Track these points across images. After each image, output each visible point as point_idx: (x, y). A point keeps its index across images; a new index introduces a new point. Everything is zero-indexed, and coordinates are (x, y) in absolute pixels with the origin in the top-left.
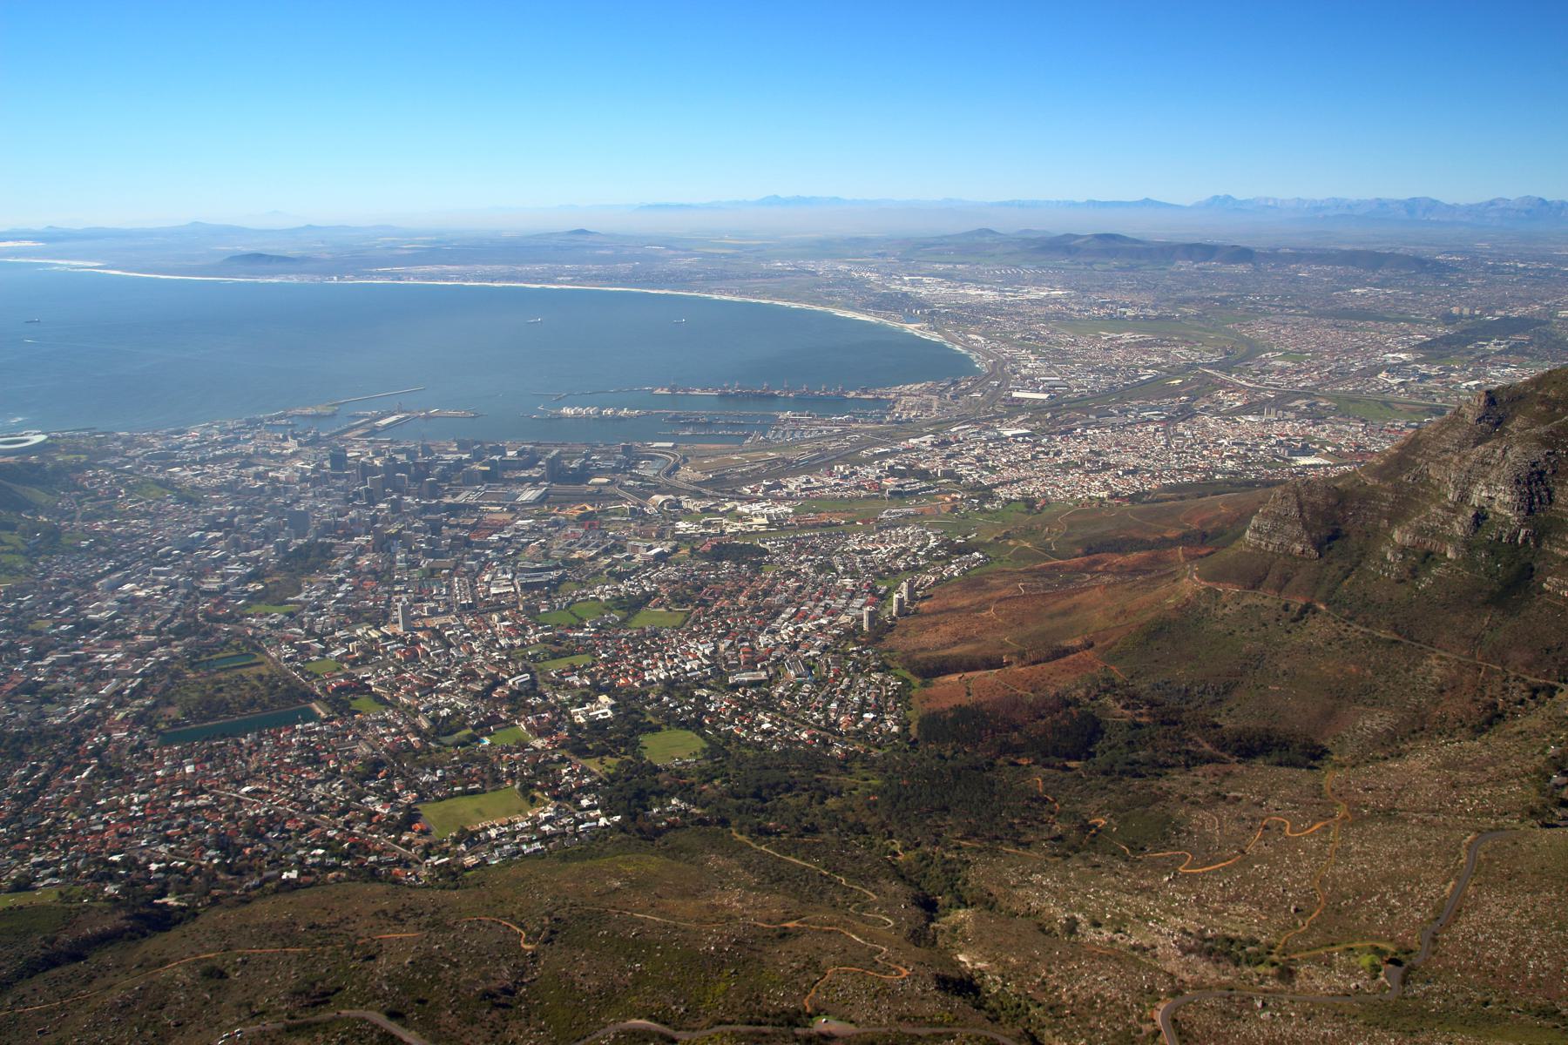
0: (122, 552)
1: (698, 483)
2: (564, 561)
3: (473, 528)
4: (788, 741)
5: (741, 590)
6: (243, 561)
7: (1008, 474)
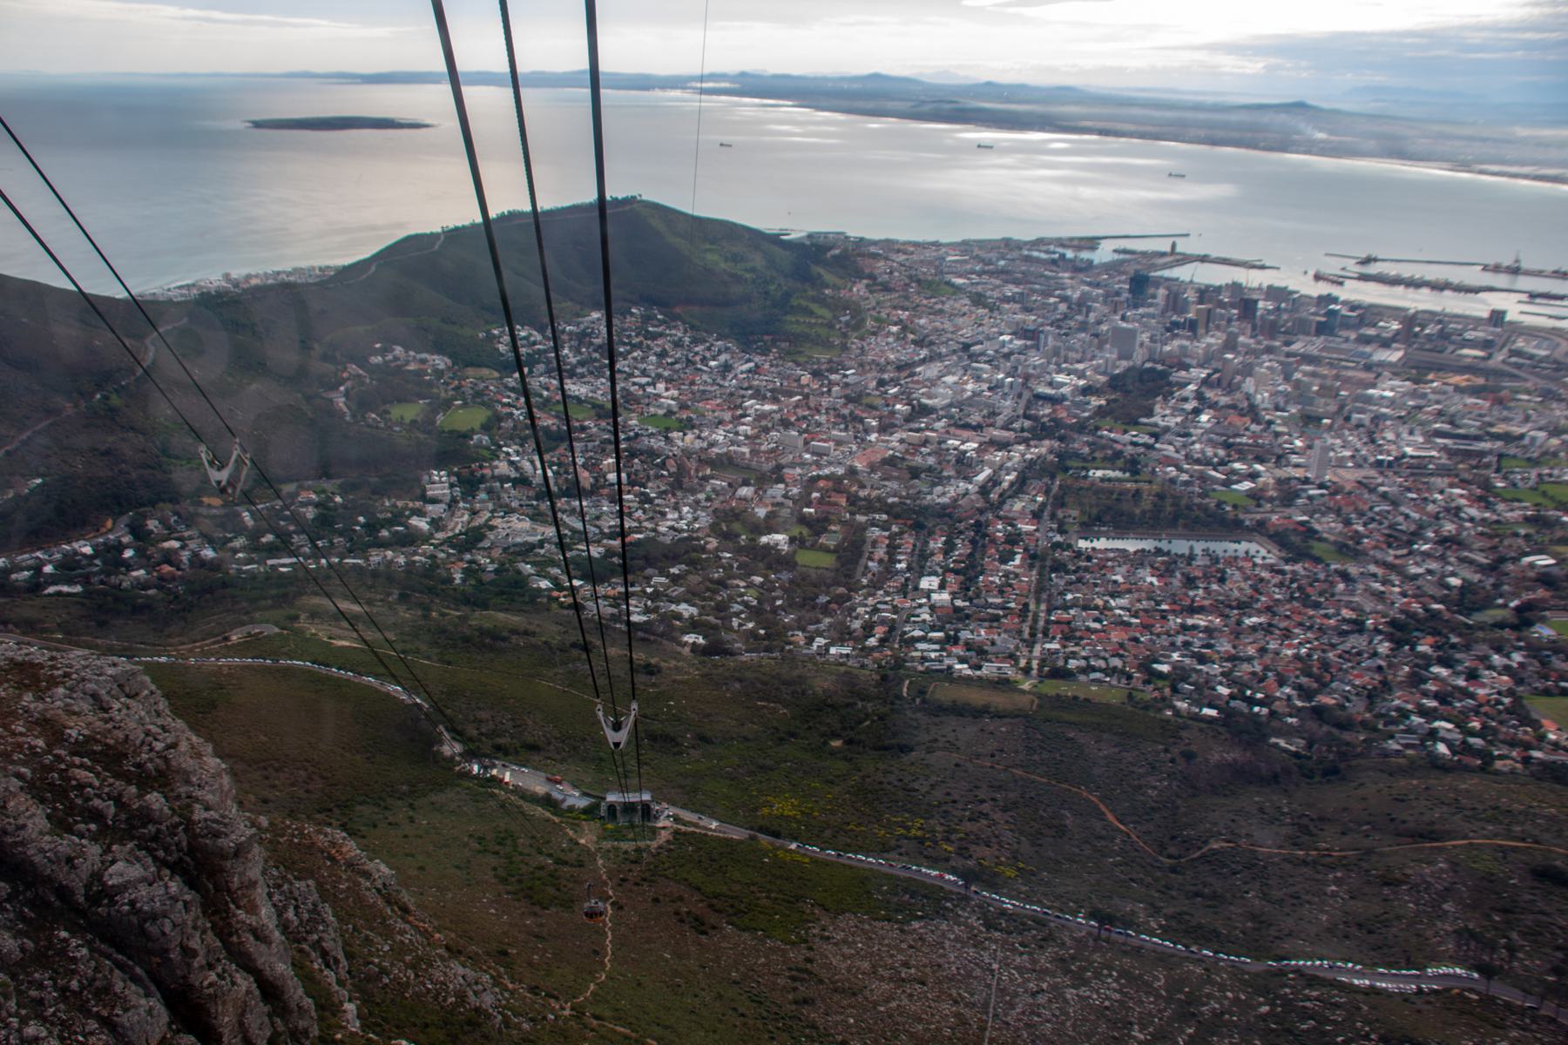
0: (932, 343)
2: (1488, 433)
3: (1337, 377)
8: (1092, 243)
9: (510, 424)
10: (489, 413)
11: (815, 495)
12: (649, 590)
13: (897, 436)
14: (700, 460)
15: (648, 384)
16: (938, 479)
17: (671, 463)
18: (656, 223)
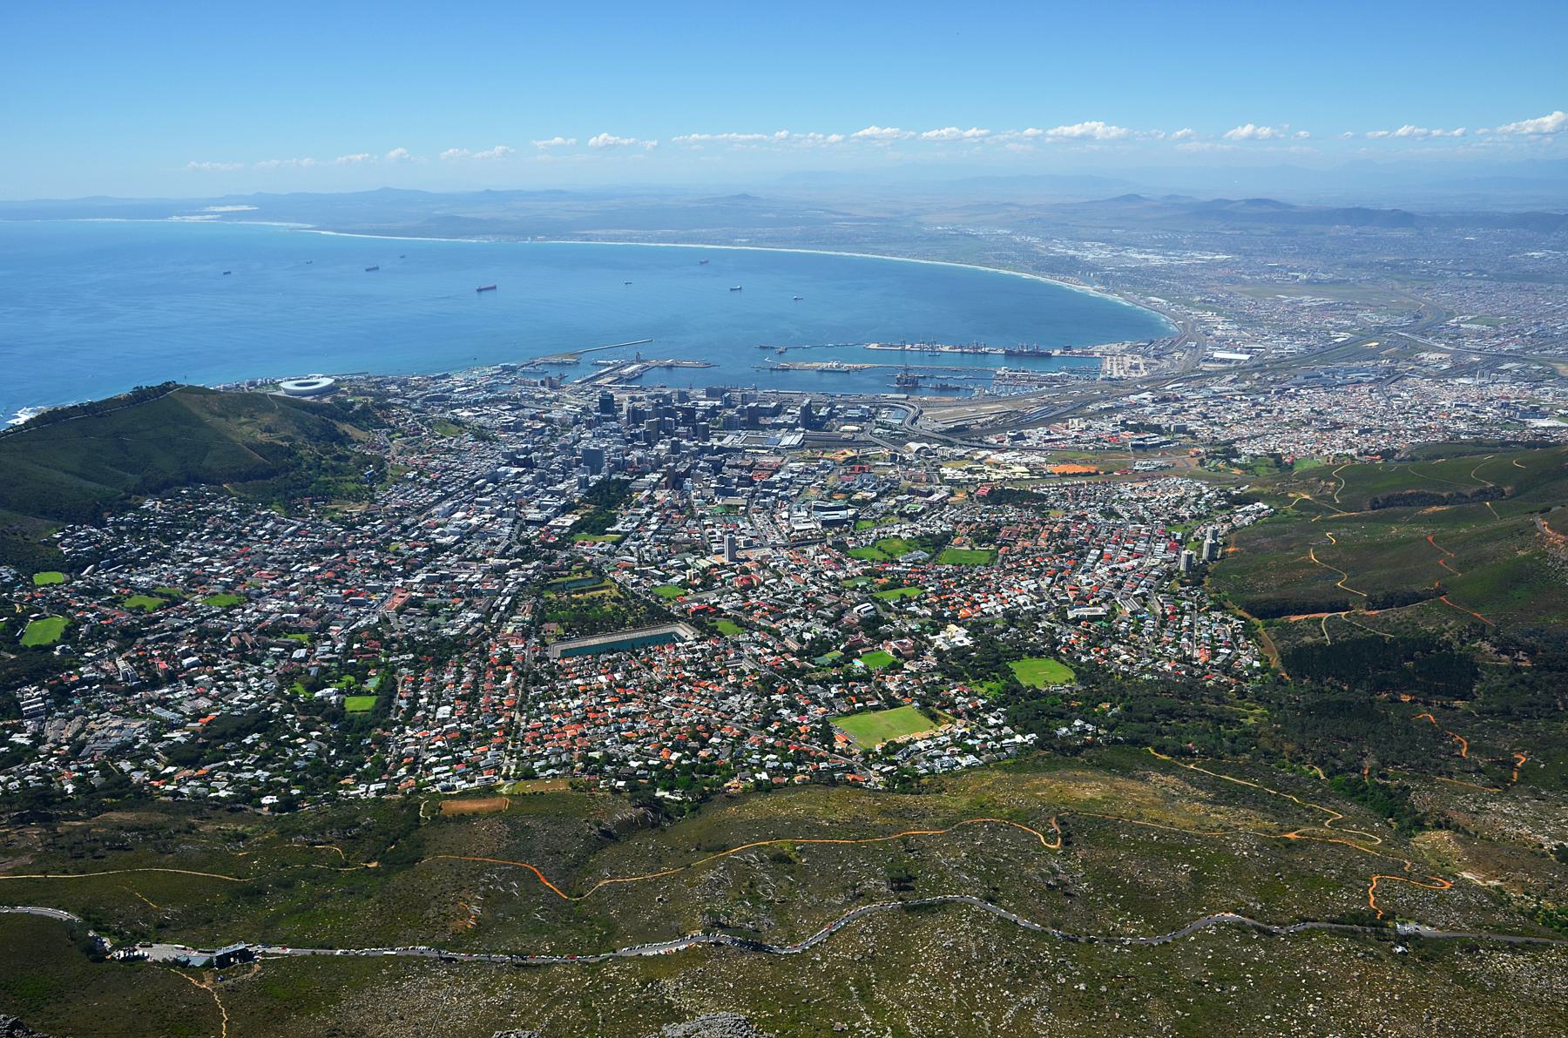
3: (750, 468)
4: (1154, 671)
5: (1035, 532)
6: (553, 494)
7: (1242, 431)
9: (84, 629)
10: (67, 621)
11: (356, 646)
12: (232, 763)
13: (418, 579)
14: (261, 632)
15: (206, 563)
16: (453, 615)
17: (234, 641)
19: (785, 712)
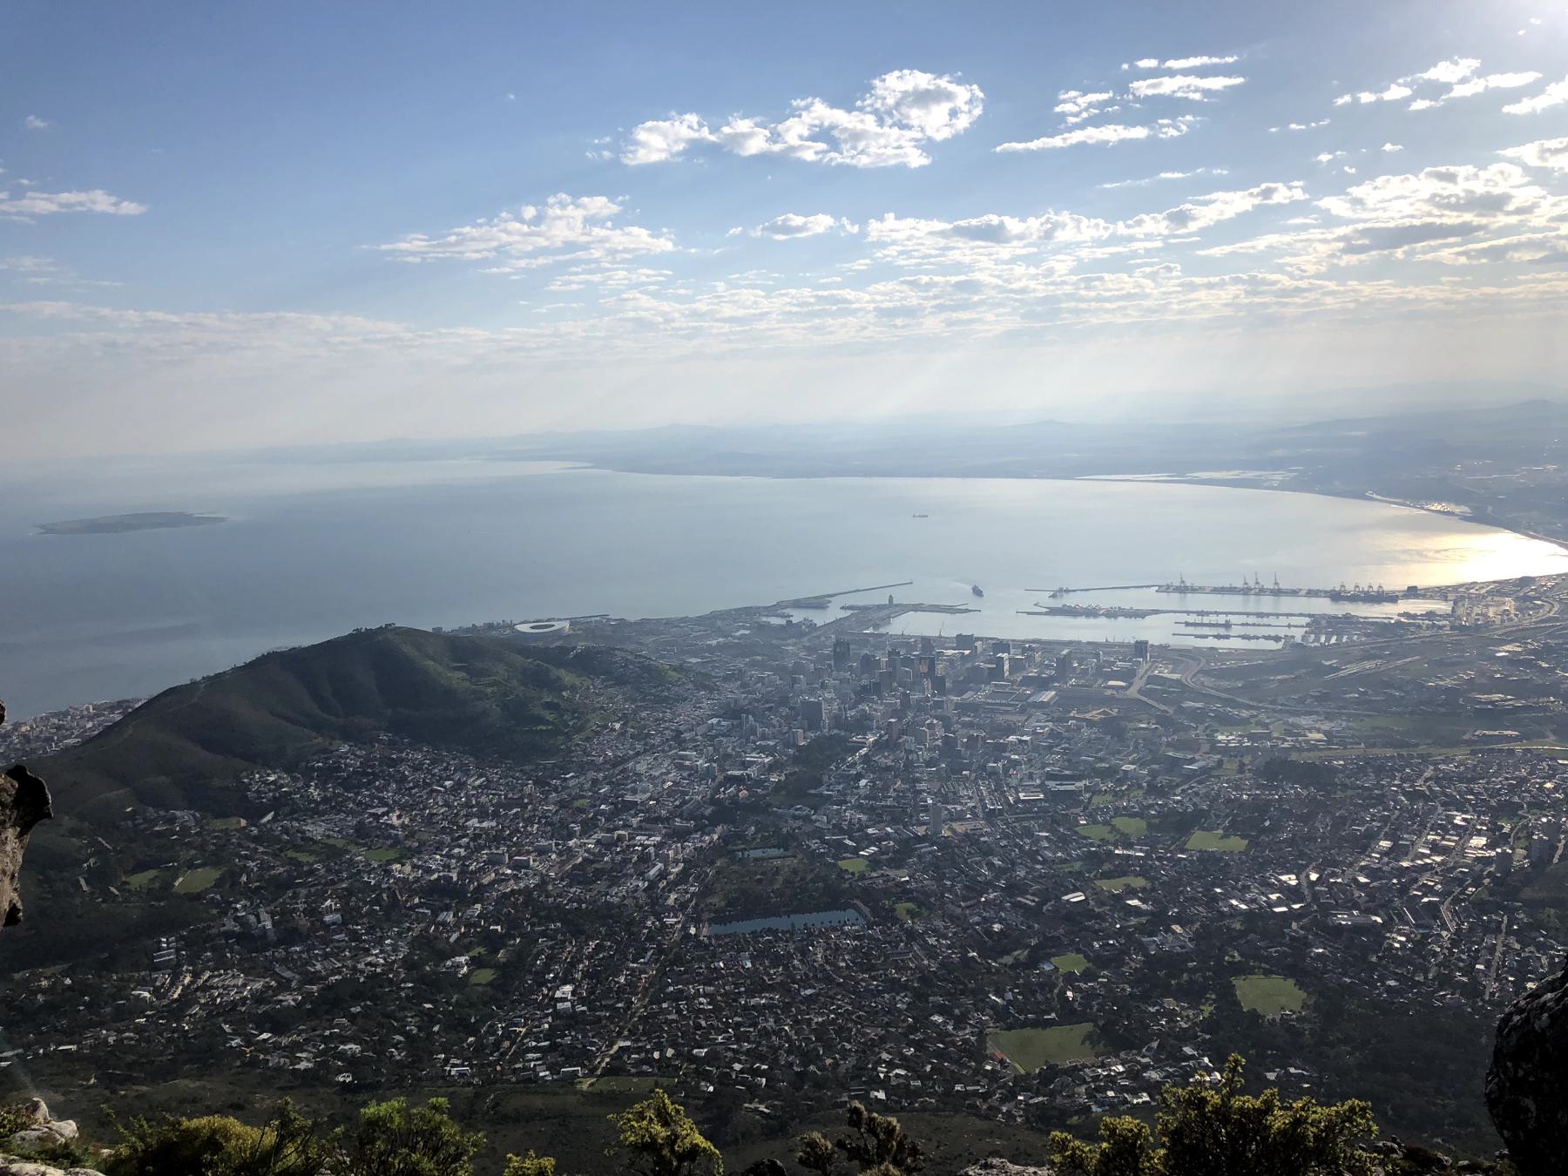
1: (1227, 690)
6: (762, 749)
8: (819, 603)
15: (384, 814)
18: (408, 650)
19: (938, 1019)
